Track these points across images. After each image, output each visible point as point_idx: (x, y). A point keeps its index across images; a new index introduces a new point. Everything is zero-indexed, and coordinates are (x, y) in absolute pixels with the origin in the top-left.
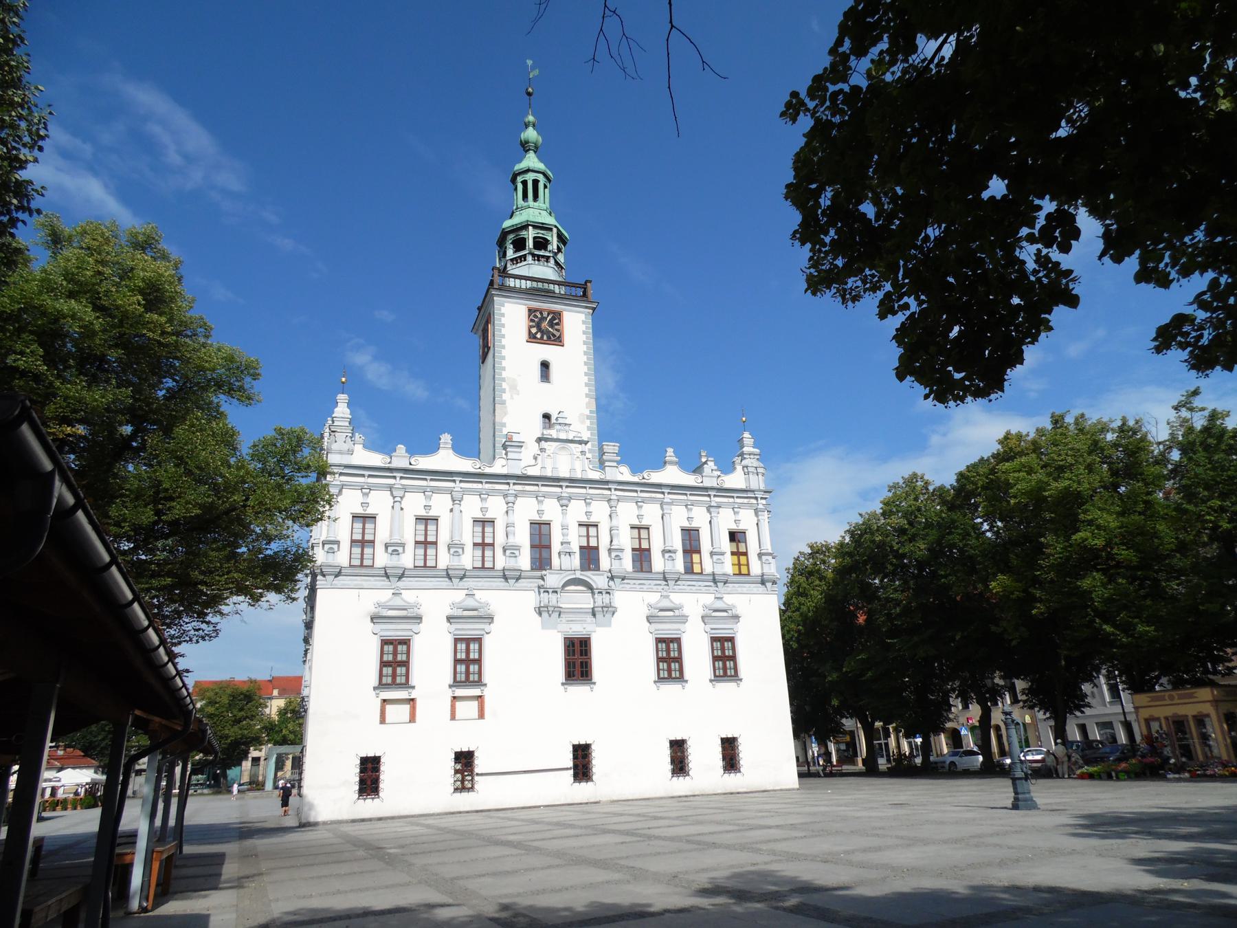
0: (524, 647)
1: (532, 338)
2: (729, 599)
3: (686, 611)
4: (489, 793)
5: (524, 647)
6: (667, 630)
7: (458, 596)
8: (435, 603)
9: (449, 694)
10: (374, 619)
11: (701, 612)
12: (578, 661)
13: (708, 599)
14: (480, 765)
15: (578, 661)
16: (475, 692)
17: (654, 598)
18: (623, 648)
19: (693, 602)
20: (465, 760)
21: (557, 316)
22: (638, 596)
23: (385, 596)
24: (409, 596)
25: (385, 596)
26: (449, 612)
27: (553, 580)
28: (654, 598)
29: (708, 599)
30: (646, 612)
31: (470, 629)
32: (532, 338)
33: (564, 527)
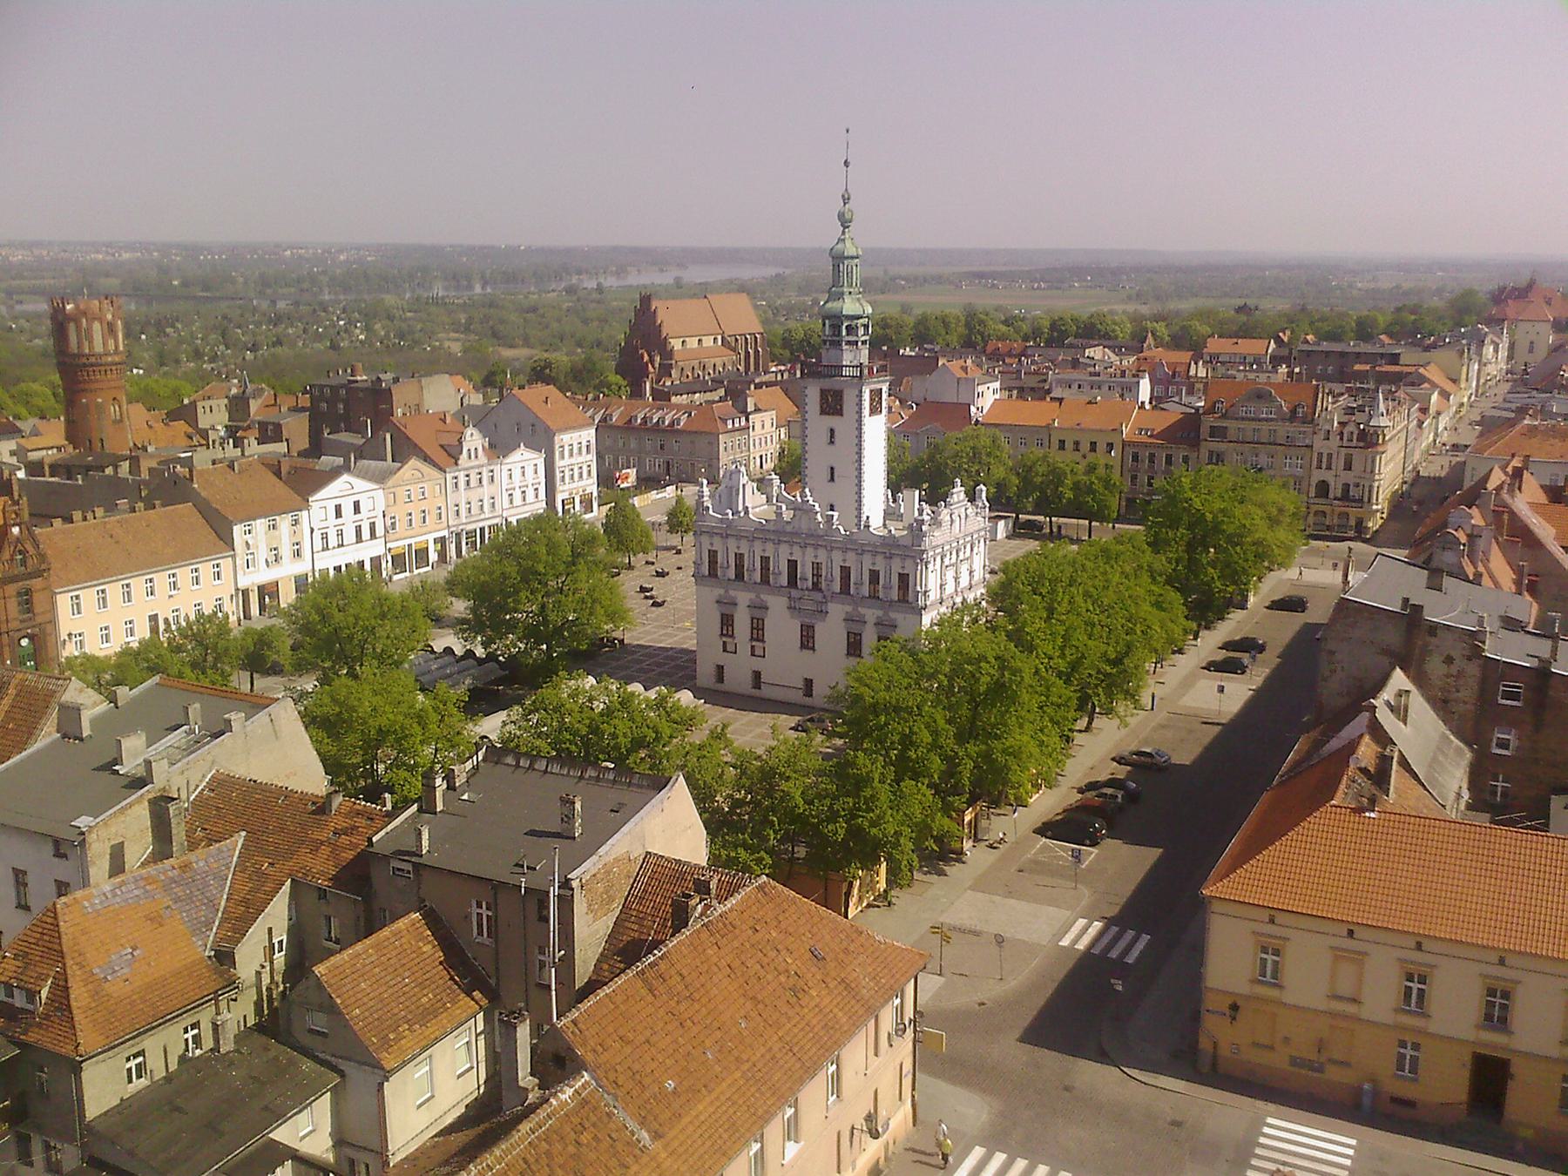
0: (782, 626)
1: (823, 412)
2: (893, 615)
5: (782, 626)
6: (855, 628)
8: (743, 598)
17: (849, 608)
18: (832, 632)
19: (871, 614)
20: (757, 675)
23: (722, 591)
24: (732, 593)
25: (722, 591)
27: (794, 593)
28: (849, 608)
29: (880, 613)
31: (758, 613)
32: (823, 412)
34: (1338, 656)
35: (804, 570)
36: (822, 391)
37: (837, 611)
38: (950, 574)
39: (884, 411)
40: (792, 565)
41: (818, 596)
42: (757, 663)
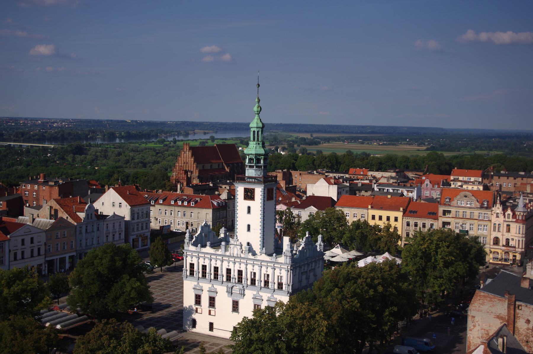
1: (245, 198)
3: (263, 298)
4: (215, 333)
7: (210, 286)
8: (206, 286)
9: (208, 309)
10: (194, 289)
11: (267, 298)
12: (235, 307)
13: (269, 295)
14: (215, 326)
15: (235, 307)
16: (213, 309)
17: (255, 293)
20: (211, 325)
21: (254, 189)
22: (251, 291)
26: (208, 289)
28: (255, 293)
29: (269, 295)
30: (252, 296)
31: (213, 295)
32: (245, 198)
33: (234, 271)
34: (476, 319)
35: (234, 274)
36: (245, 189)
37: (250, 293)
38: (304, 277)
39: (274, 199)
40: (229, 271)
41: (240, 286)
42: (211, 319)
